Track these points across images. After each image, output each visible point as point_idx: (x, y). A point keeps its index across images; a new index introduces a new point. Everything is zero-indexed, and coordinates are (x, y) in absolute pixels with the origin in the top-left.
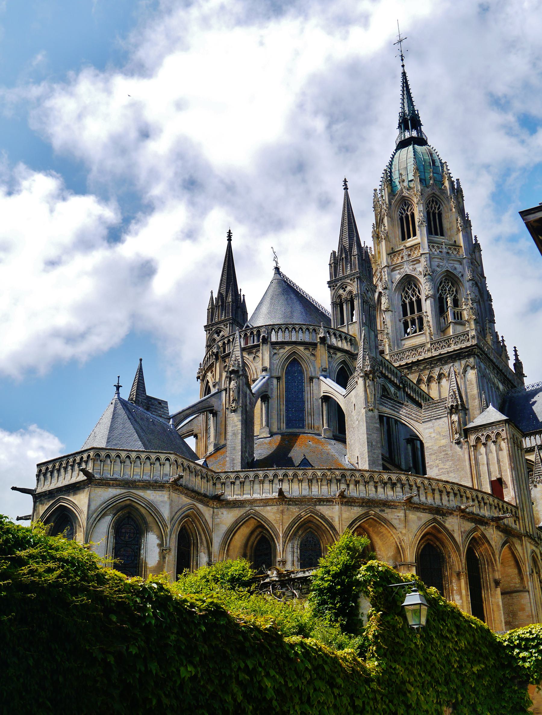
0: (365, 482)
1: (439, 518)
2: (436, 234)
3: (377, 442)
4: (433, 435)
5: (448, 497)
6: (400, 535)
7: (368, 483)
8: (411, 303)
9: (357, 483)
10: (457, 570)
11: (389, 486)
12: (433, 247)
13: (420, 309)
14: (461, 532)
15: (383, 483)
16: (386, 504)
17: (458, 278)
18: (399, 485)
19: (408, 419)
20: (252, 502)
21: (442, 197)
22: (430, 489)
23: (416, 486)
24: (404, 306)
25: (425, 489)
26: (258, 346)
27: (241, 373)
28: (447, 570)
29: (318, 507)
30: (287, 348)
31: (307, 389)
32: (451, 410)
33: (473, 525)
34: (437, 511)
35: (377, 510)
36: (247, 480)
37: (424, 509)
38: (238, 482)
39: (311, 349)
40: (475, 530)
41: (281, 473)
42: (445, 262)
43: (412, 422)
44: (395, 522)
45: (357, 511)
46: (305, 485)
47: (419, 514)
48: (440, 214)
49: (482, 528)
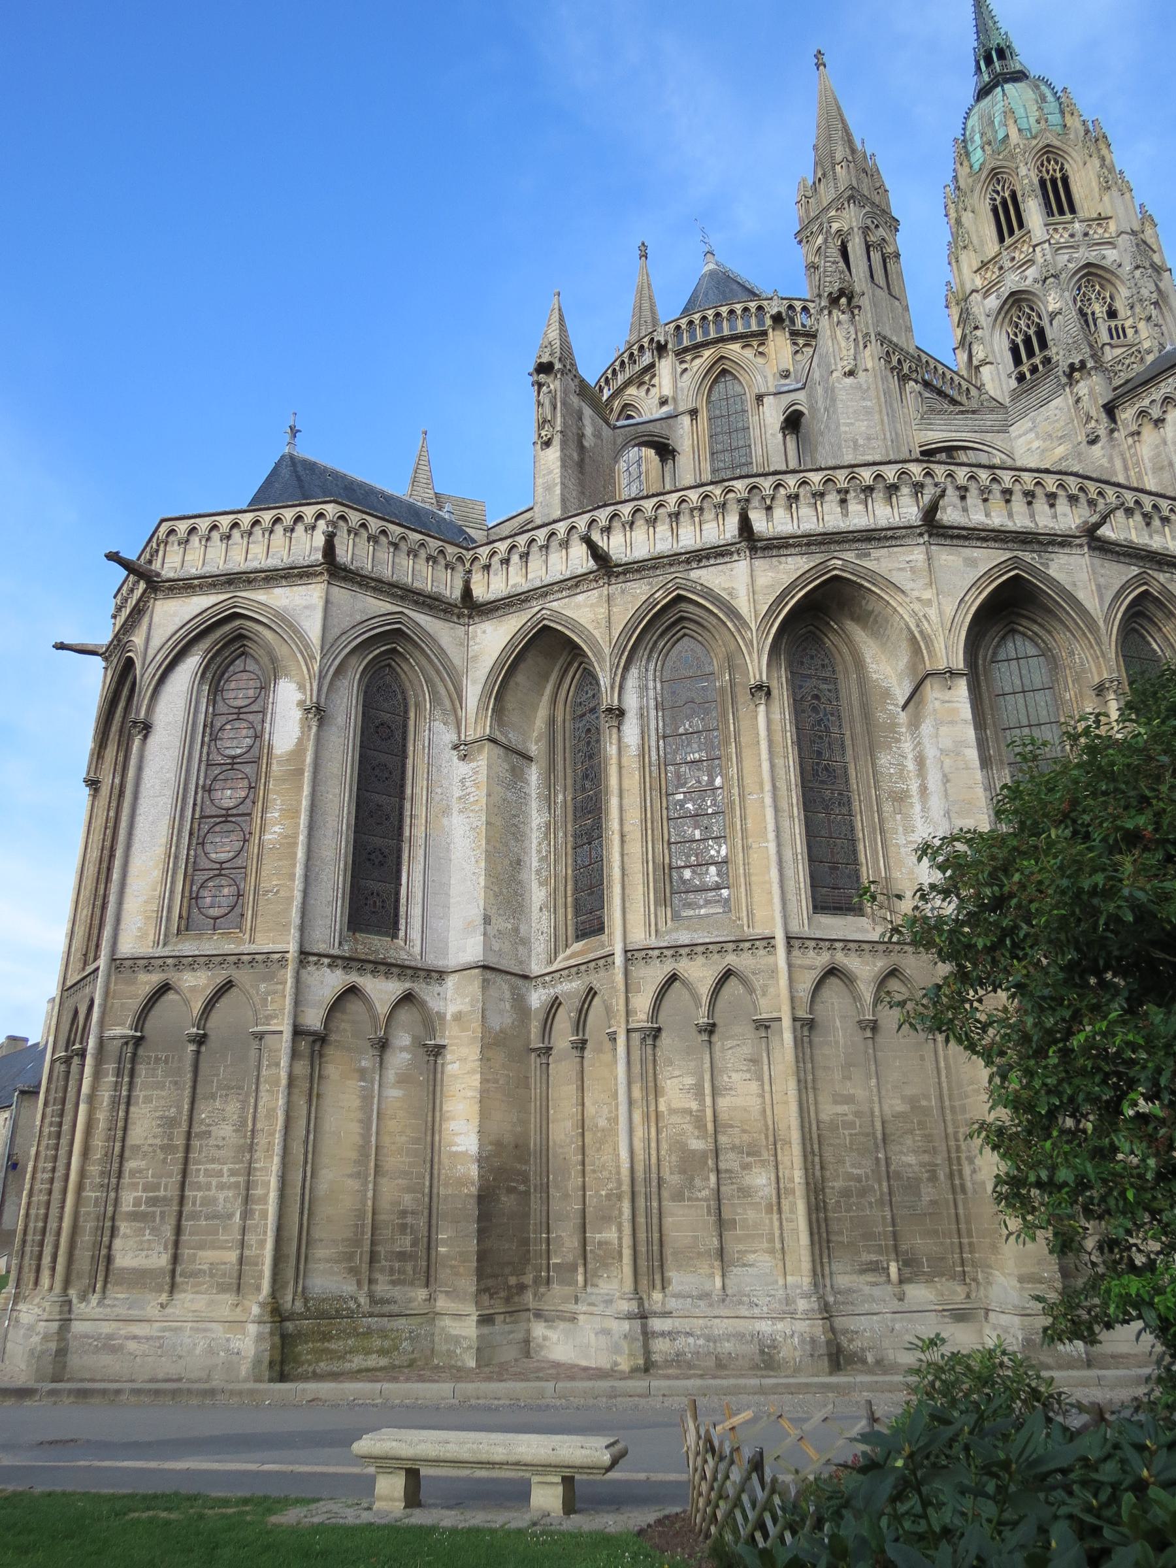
0: (814, 495)
1: (1027, 557)
2: (1062, 212)
3: (869, 439)
4: (1036, 444)
5: (1052, 506)
6: (916, 606)
7: (822, 495)
8: (1027, 341)
9: (794, 498)
10: (1097, 680)
11: (878, 495)
12: (1056, 230)
13: (1044, 345)
14: (1099, 586)
15: (863, 491)
16: (871, 537)
17: (1113, 273)
18: (905, 490)
19: (978, 435)
20: (544, 591)
21: (1065, 147)
22: (998, 495)
23: (958, 488)
24: (1015, 350)
25: (982, 492)
26: (652, 366)
27: (558, 366)
28: (1067, 688)
29: (694, 575)
30: (707, 353)
31: (753, 420)
32: (1070, 376)
33: (1135, 570)
34: (1026, 539)
35: (850, 556)
36: (534, 548)
37: (985, 539)
38: (515, 558)
39: (755, 344)
40: (1139, 579)
41: (603, 515)
42: (1082, 250)
43: (988, 437)
44: (896, 578)
45: (794, 566)
46: (663, 529)
47: (967, 552)
48: (1065, 180)
49: (1162, 577)
